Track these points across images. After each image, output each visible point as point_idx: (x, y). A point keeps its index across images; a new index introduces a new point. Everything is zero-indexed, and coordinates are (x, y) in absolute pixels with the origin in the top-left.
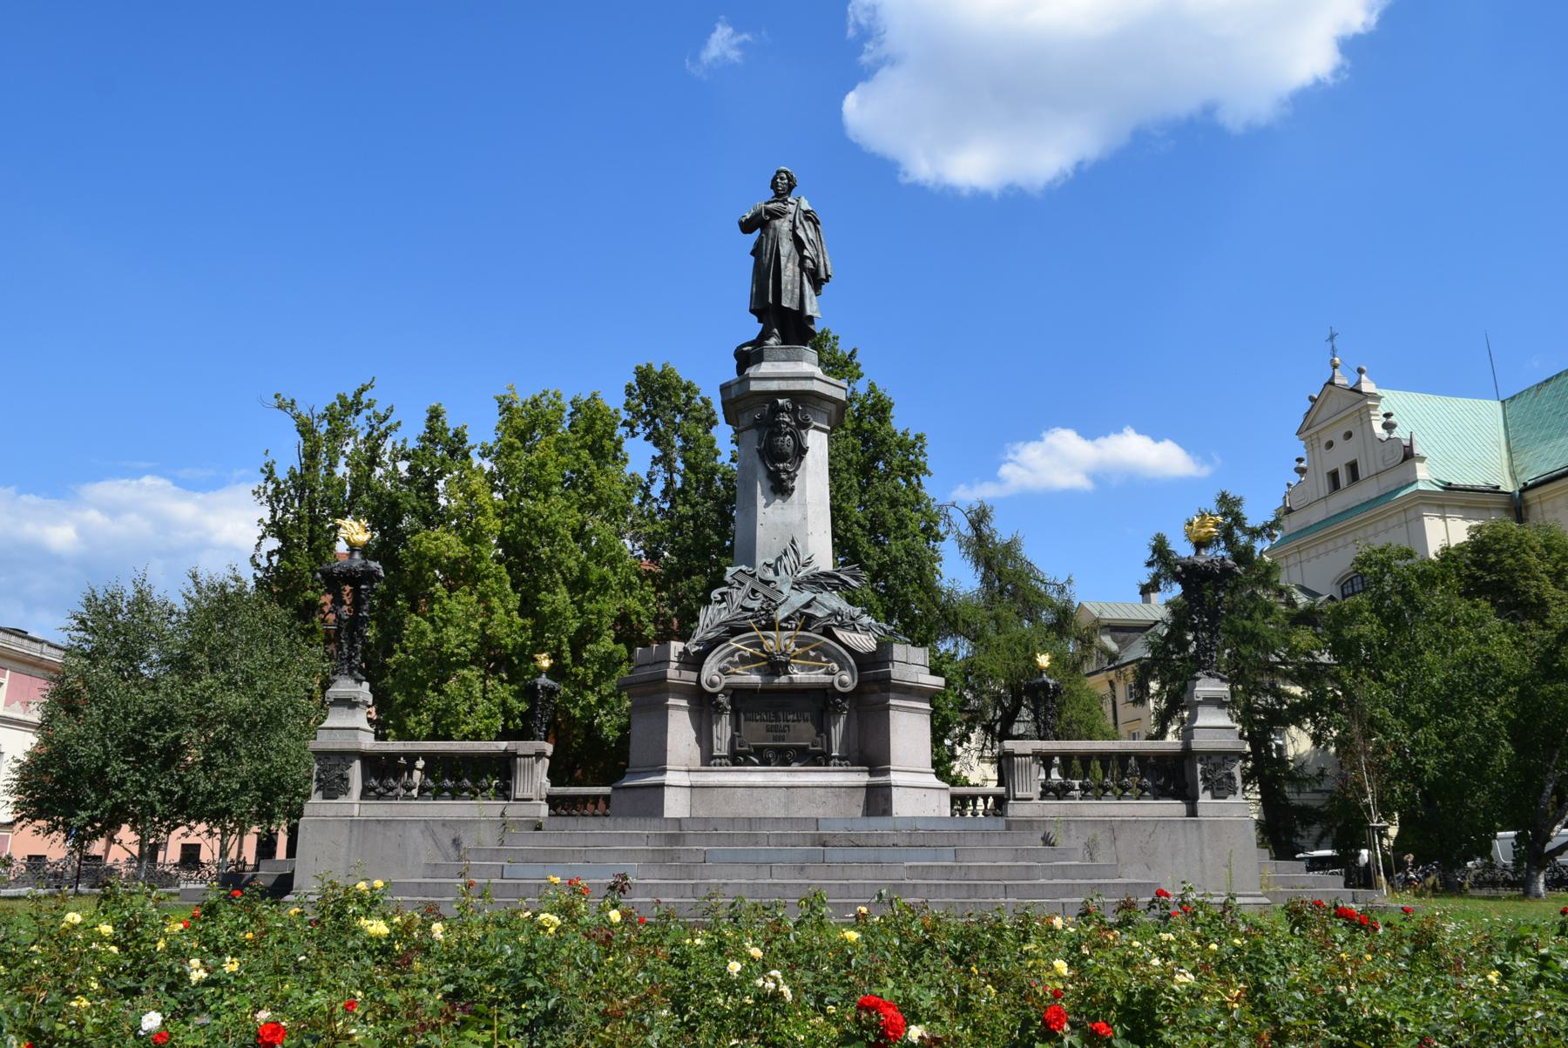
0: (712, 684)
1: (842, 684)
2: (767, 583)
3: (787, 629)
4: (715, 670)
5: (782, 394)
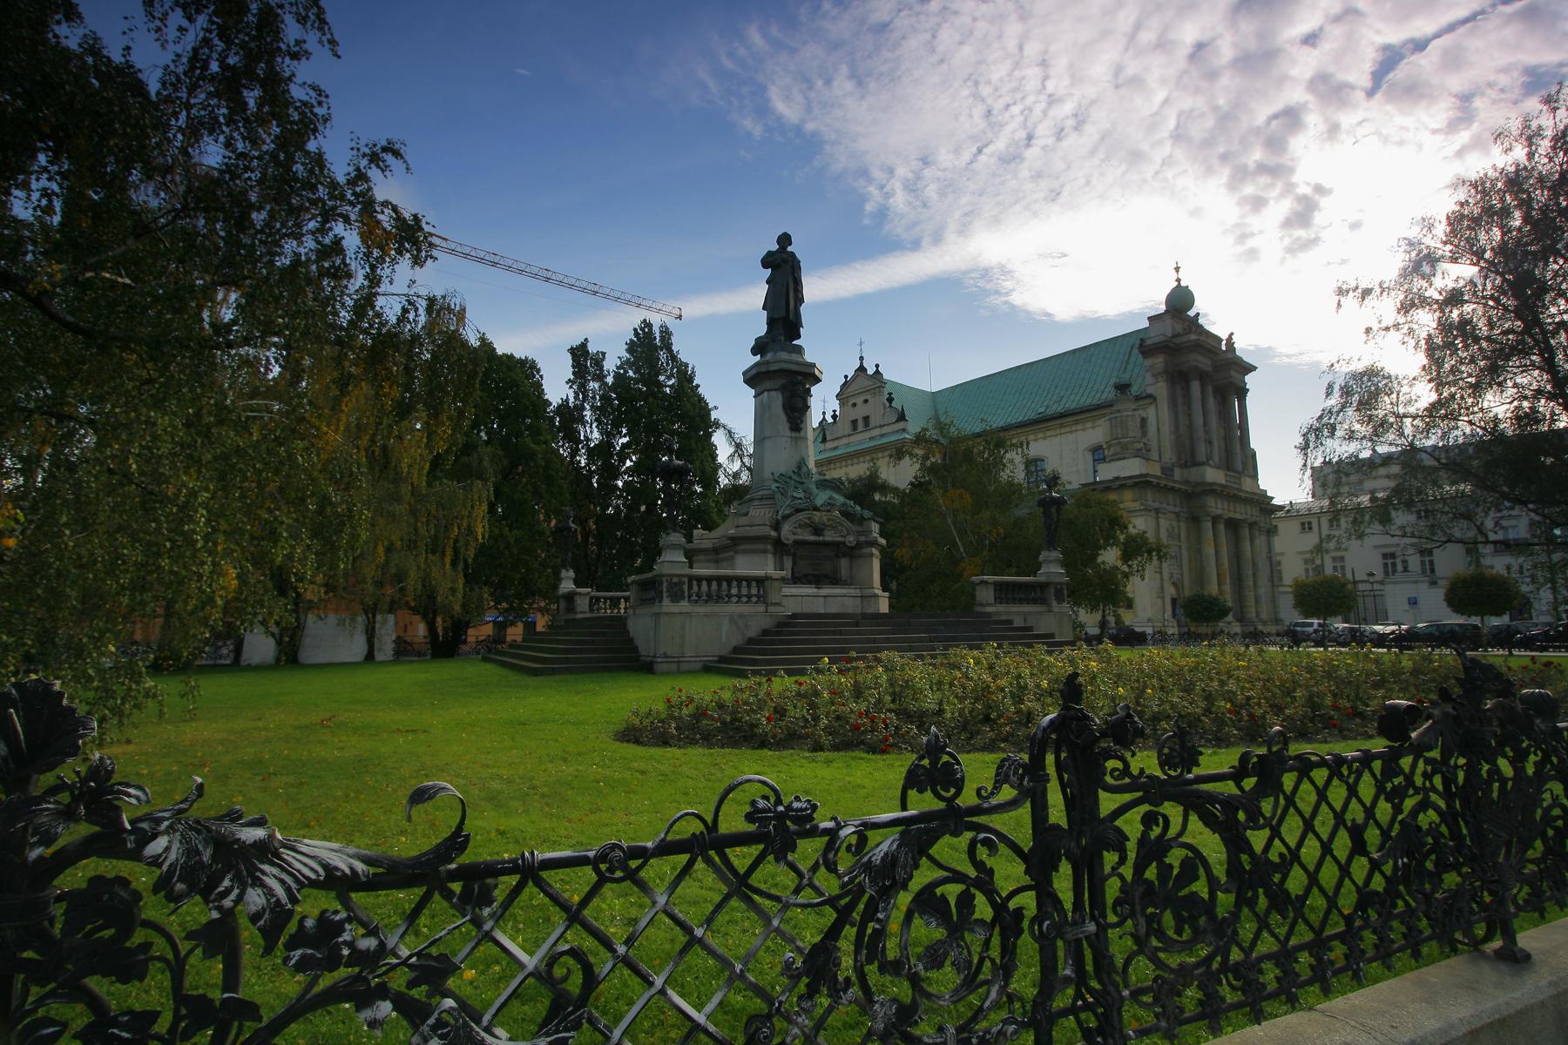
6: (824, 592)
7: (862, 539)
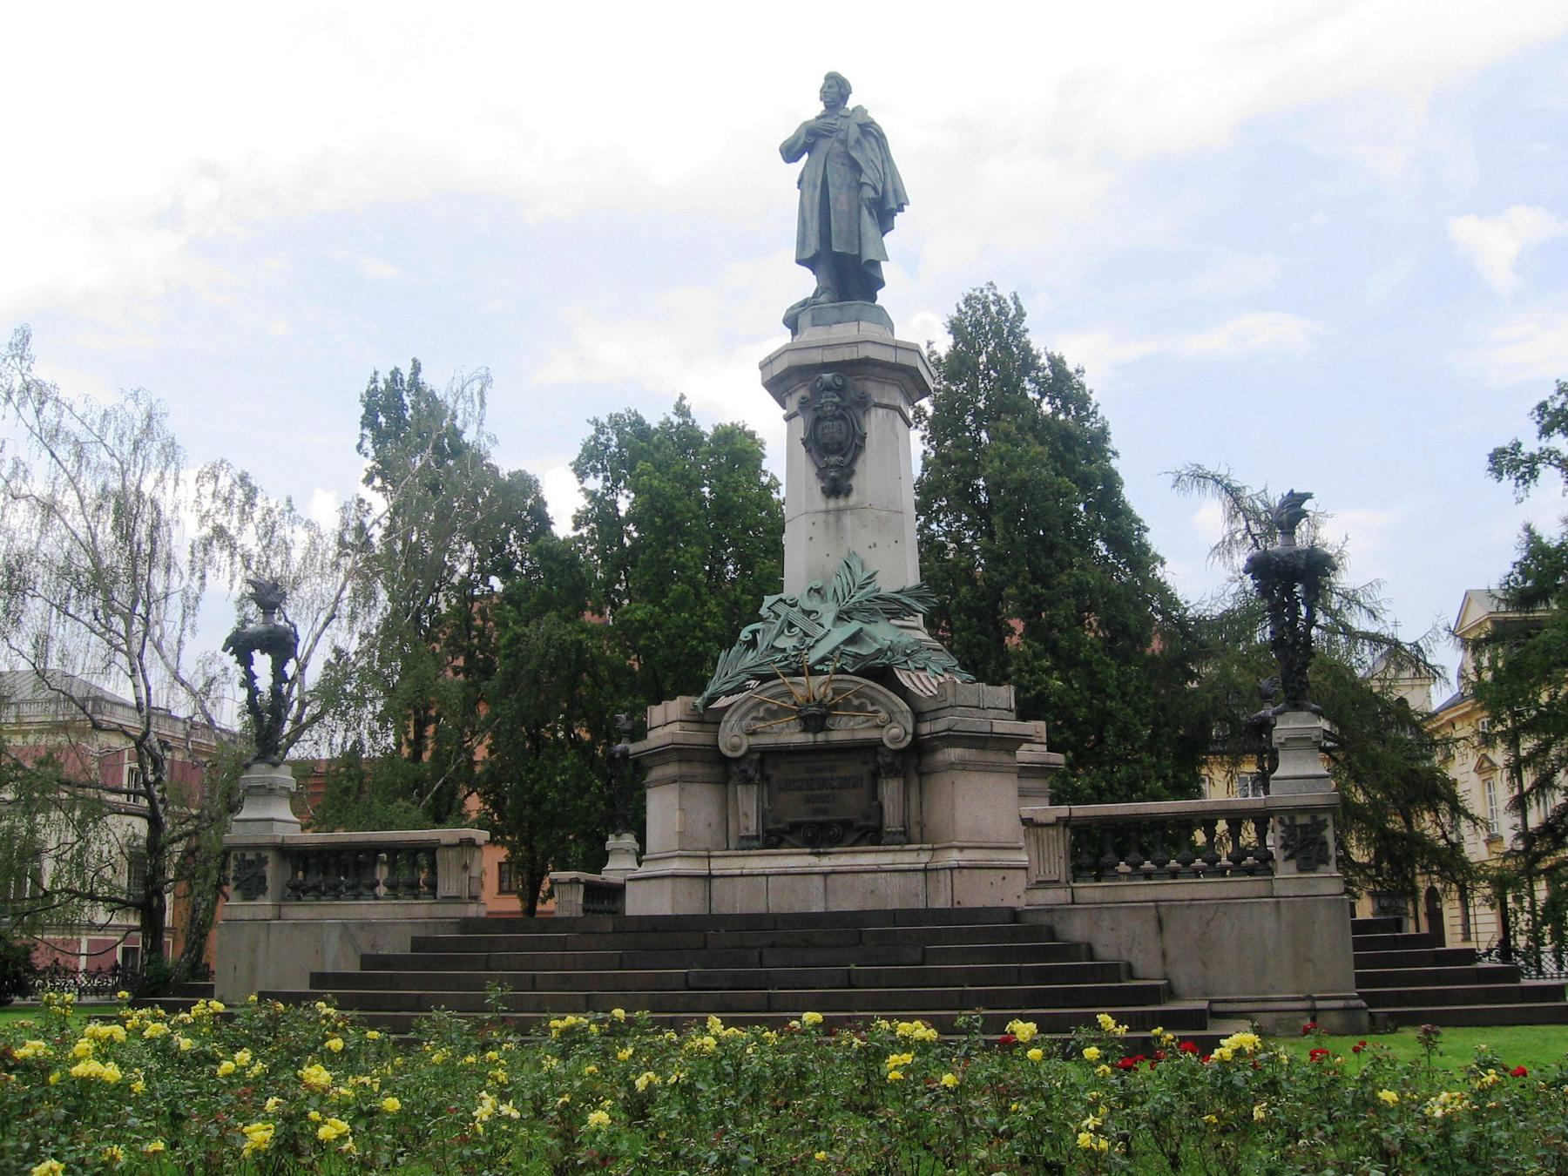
0: (735, 748)
1: (895, 739)
2: (808, 613)
3: (822, 673)
4: (736, 731)
5: (826, 367)
6: (826, 863)
7: (926, 728)
